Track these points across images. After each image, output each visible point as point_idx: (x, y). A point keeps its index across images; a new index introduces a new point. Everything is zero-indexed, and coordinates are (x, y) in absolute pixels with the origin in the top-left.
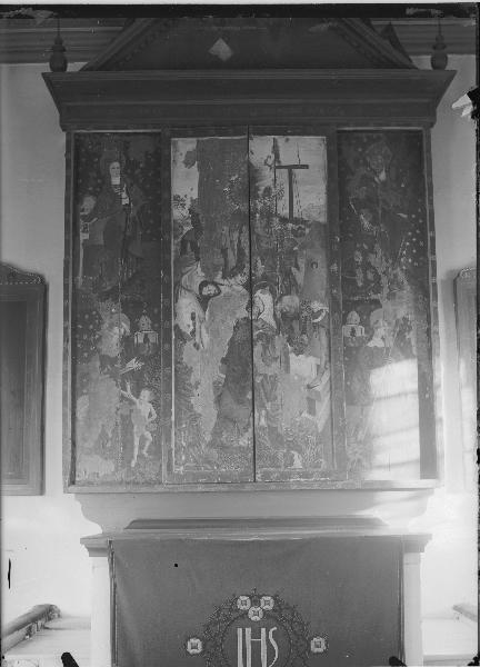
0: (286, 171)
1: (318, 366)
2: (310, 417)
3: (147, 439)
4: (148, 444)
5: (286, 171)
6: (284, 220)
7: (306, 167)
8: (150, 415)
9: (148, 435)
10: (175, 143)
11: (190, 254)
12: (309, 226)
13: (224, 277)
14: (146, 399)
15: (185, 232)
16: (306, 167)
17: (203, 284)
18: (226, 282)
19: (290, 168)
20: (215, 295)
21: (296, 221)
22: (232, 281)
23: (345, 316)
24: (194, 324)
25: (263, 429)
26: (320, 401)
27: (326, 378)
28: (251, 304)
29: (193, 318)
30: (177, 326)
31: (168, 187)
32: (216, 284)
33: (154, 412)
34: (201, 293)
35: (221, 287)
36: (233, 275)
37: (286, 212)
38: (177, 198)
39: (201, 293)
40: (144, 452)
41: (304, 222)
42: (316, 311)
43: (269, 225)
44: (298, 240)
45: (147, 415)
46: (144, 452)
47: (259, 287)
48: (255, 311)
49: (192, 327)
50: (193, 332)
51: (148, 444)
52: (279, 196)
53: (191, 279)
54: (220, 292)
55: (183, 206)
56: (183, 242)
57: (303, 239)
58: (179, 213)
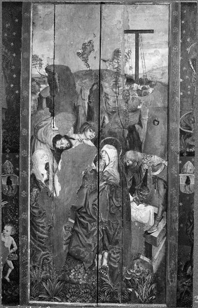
0: (134, 35)
1: (155, 215)
2: (146, 259)
3: (9, 267)
4: (10, 271)
5: (134, 35)
6: (130, 80)
7: (151, 31)
8: (12, 247)
9: (10, 263)
10: (35, 8)
11: (46, 110)
12: (151, 86)
13: (75, 132)
14: (9, 233)
15: (41, 89)
16: (151, 31)
17: (58, 137)
18: (76, 136)
19: (137, 32)
20: (67, 148)
21: (141, 82)
22: (82, 136)
23: (181, 166)
24: (48, 173)
25: (104, 268)
26: (156, 245)
27: (162, 225)
28: (99, 157)
29: (47, 168)
30: (33, 176)
31: (28, 49)
32: (67, 138)
33: (14, 243)
34: (54, 145)
35: (73, 142)
36: (83, 131)
37: (132, 72)
38: (35, 58)
39: (54, 145)
40: (7, 278)
41: (149, 82)
42: (156, 164)
43: (116, 84)
44: (142, 98)
45: (9, 247)
46: (7, 278)
47: (106, 142)
48: (102, 163)
49: (45, 177)
50: (47, 181)
51: (10, 271)
52: (127, 58)
53: (46, 134)
54: (71, 146)
55: (41, 65)
56: (40, 99)
57: (146, 98)
58: (37, 71)
